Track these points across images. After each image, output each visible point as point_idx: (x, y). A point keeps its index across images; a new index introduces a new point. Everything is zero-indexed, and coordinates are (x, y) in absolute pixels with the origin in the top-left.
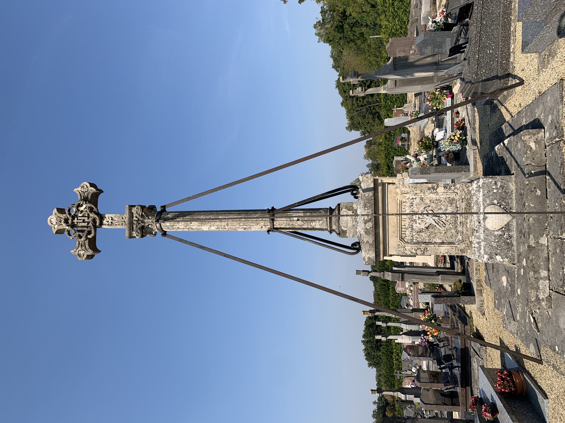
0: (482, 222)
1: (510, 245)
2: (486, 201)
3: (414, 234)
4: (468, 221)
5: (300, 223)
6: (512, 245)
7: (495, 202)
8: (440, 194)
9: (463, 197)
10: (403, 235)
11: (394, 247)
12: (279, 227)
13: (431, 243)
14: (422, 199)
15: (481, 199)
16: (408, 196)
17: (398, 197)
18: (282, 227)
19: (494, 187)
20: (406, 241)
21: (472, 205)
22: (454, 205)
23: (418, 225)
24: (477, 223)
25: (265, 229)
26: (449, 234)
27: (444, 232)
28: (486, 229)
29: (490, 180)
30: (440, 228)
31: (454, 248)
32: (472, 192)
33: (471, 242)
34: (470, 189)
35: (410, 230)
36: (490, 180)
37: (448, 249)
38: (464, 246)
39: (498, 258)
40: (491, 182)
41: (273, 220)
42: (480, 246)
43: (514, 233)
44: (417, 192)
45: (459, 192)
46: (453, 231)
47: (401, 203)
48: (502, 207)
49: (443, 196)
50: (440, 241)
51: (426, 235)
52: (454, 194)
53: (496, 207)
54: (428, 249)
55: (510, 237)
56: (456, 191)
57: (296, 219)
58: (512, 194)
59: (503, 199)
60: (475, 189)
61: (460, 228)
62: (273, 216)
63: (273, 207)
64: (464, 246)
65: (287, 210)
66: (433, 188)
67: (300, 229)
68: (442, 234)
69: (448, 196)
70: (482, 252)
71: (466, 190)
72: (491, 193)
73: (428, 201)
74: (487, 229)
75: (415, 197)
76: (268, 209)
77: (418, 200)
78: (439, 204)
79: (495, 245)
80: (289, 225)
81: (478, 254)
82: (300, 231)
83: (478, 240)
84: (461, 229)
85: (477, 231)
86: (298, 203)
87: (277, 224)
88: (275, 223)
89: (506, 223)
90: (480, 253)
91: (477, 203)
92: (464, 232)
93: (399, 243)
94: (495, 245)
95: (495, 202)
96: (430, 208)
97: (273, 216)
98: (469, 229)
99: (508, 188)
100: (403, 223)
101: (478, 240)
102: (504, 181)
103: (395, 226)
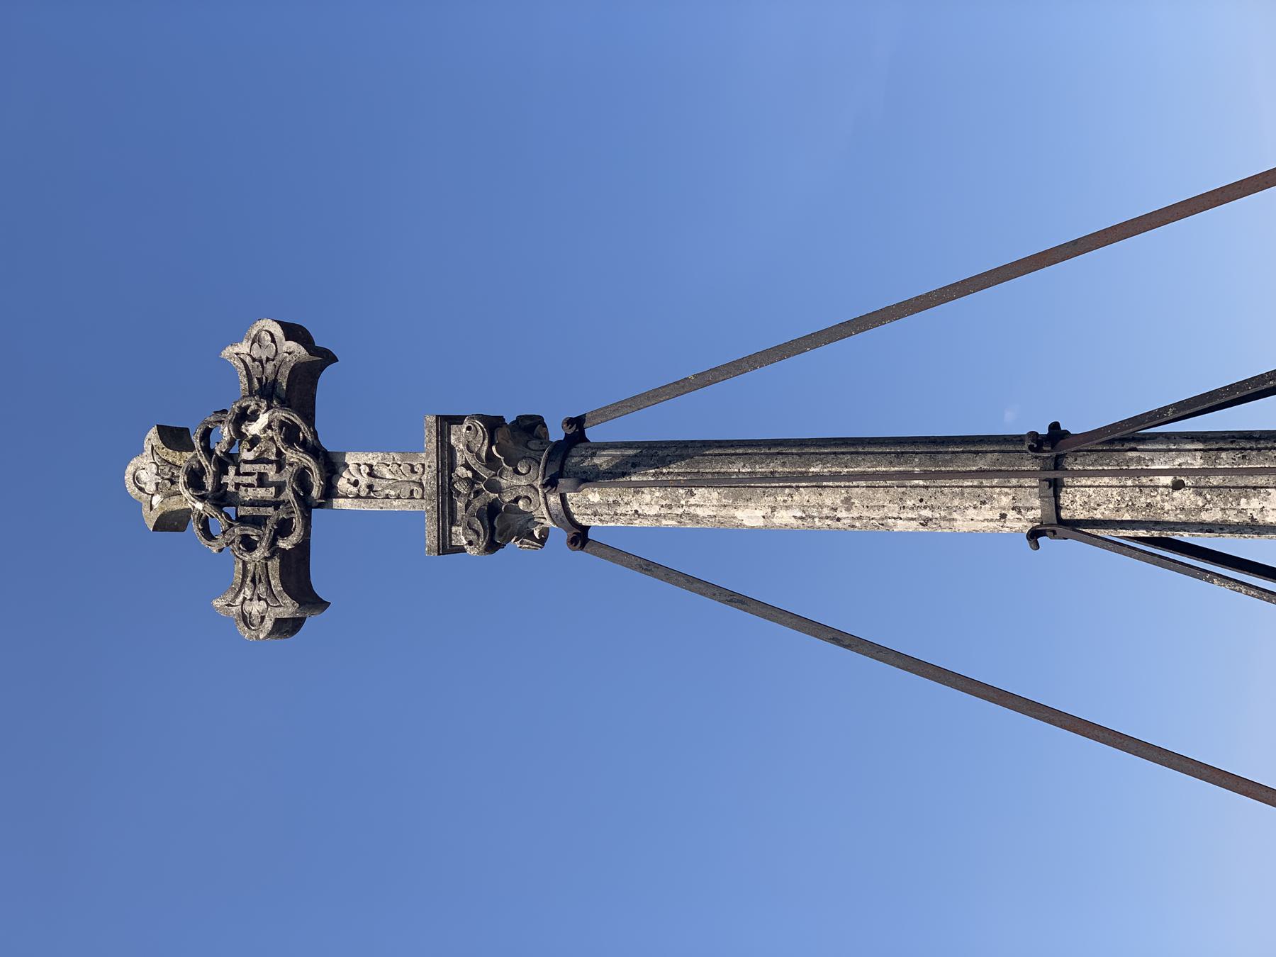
5: (1185, 497)
12: (1082, 515)
18: (1098, 516)
25: (1019, 524)
41: (1056, 486)
57: (1168, 480)
62: (1057, 466)
63: (1054, 426)
65: (1122, 440)
67: (1184, 526)
76: (1034, 435)
80: (1132, 507)
82: (1185, 537)
86: (1179, 406)
87: (1075, 503)
88: (1065, 499)
97: (1057, 466)
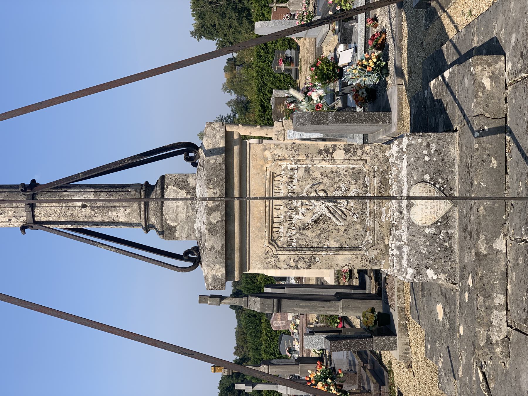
0: (405, 211)
1: (448, 251)
2: (412, 176)
3: (294, 232)
4: (383, 209)
5: (87, 211)
6: (453, 252)
7: (427, 177)
8: (338, 162)
9: (376, 168)
12: (44, 219)
14: (307, 170)
15: (404, 172)
16: (284, 164)
17: (268, 166)
18: (51, 219)
19: (425, 152)
20: (280, 244)
22: (361, 182)
23: (300, 217)
24: (397, 214)
25: (17, 223)
27: (343, 229)
28: (411, 224)
29: (420, 140)
30: (338, 223)
31: (359, 256)
32: (391, 160)
33: (387, 247)
34: (388, 154)
35: (286, 225)
36: (420, 140)
38: (375, 252)
40: (421, 144)
41: (33, 207)
42: (401, 254)
43: (455, 232)
44: (300, 158)
45: (368, 159)
46: (358, 227)
47: (273, 175)
48: (437, 186)
51: (314, 234)
52: (361, 162)
53: (429, 186)
56: (364, 157)
57: (80, 204)
58: (454, 164)
59: (439, 172)
61: (369, 223)
62: (33, 198)
63: (33, 181)
64: (375, 252)
65: (61, 187)
67: (87, 223)
68: (341, 233)
69: (351, 166)
70: (405, 262)
72: (421, 162)
73: (317, 174)
74: (413, 224)
76: (23, 185)
77: (301, 173)
78: (336, 179)
80: (65, 216)
81: (398, 267)
82: (87, 227)
83: (398, 243)
84: (371, 223)
86: (84, 173)
87: (41, 214)
88: (37, 212)
89: (443, 213)
90: (401, 265)
91: (398, 179)
92: (377, 229)
95: (427, 177)
96: (322, 187)
97: (33, 198)
98: (384, 224)
99: (447, 154)
101: (398, 243)
103: (261, 219)
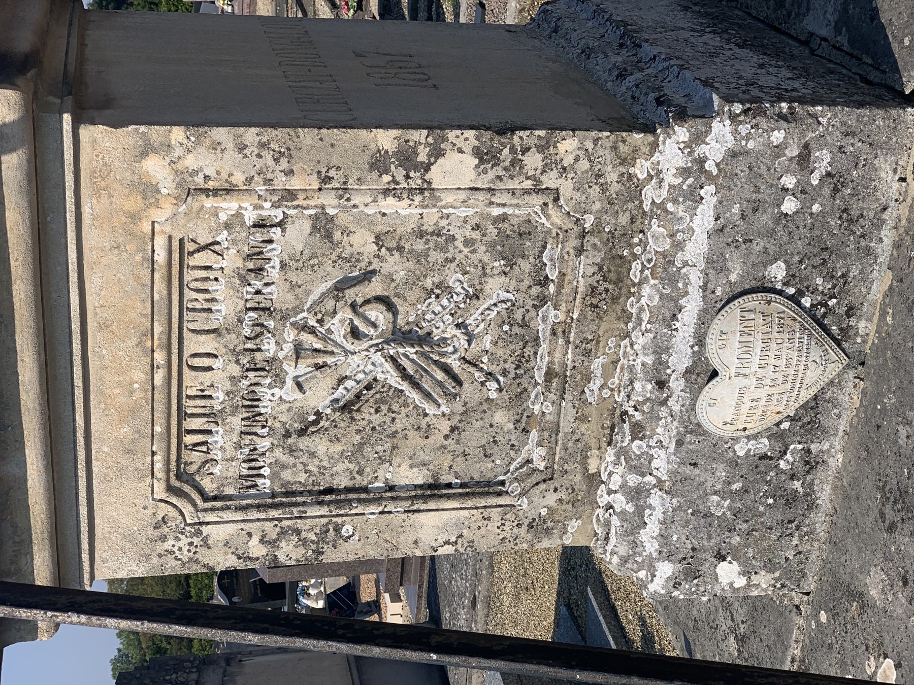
0: (676, 384)
1: (796, 505)
2: (723, 270)
3: (264, 444)
4: (597, 364)
6: (812, 506)
7: (778, 272)
8: (448, 198)
9: (589, 221)
10: (187, 456)
11: (131, 538)
13: (359, 493)
14: (323, 226)
15: (696, 248)
16: (228, 206)
17: (159, 215)
19: (789, 181)
20: (208, 485)
21: (635, 273)
22: (525, 265)
23: (289, 392)
24: (644, 388)
26: (474, 437)
27: (445, 426)
28: (692, 428)
29: (777, 137)
30: (430, 409)
31: (495, 514)
32: (650, 194)
33: (594, 480)
34: (640, 170)
35: (237, 422)
36: (777, 137)
37: (460, 524)
38: (551, 499)
39: (729, 574)
40: (779, 149)
42: (640, 512)
43: (834, 451)
44: (296, 183)
45: (566, 187)
46: (500, 417)
47: (182, 250)
48: (806, 302)
49: (463, 212)
50: (419, 477)
51: (338, 448)
52: (537, 201)
53: (779, 305)
54: (347, 530)
55: (811, 463)
56: (550, 180)
58: (879, 223)
59: (822, 254)
60: (670, 179)
61: (540, 405)
64: (551, 499)
66: (407, 158)
68: (437, 439)
69: (496, 211)
70: (649, 538)
71: (612, 176)
72: (765, 219)
73: (362, 242)
74: (698, 430)
75: (278, 215)
77: (296, 236)
78: (436, 257)
79: (719, 506)
81: (623, 550)
83: (633, 480)
84: (549, 409)
85: (638, 432)
89: (806, 395)
90: (634, 545)
91: (667, 269)
92: (567, 423)
93: (164, 509)
94: (719, 506)
95: (778, 272)
96: (376, 287)
98: (593, 413)
99: (867, 187)
100: (193, 382)
101: (633, 480)
102: (854, 146)
103: (134, 411)
